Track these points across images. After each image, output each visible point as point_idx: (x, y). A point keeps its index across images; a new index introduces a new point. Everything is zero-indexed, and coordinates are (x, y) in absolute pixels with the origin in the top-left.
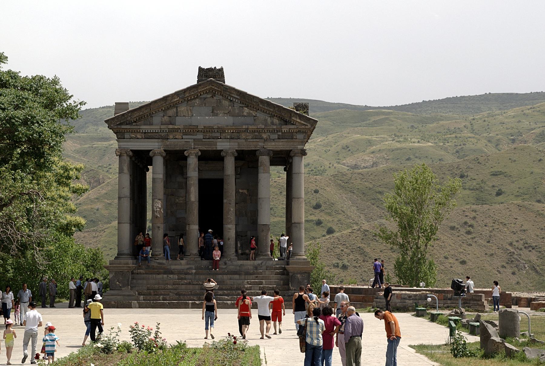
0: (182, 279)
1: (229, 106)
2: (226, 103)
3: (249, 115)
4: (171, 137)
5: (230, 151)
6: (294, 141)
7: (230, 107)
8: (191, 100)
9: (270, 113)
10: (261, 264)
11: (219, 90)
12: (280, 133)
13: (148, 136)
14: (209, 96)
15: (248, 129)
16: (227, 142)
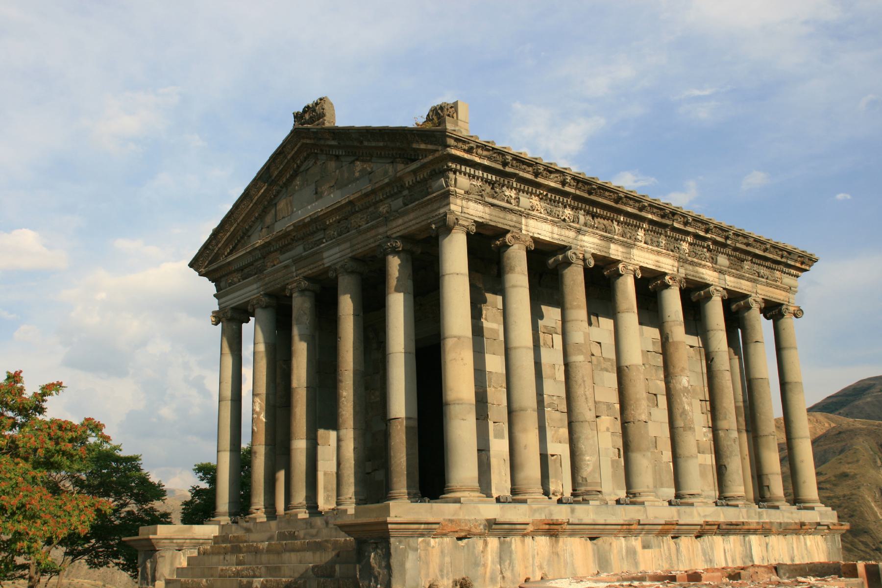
2: (332, 165)
5: (339, 265)
12: (406, 192)
15: (351, 203)
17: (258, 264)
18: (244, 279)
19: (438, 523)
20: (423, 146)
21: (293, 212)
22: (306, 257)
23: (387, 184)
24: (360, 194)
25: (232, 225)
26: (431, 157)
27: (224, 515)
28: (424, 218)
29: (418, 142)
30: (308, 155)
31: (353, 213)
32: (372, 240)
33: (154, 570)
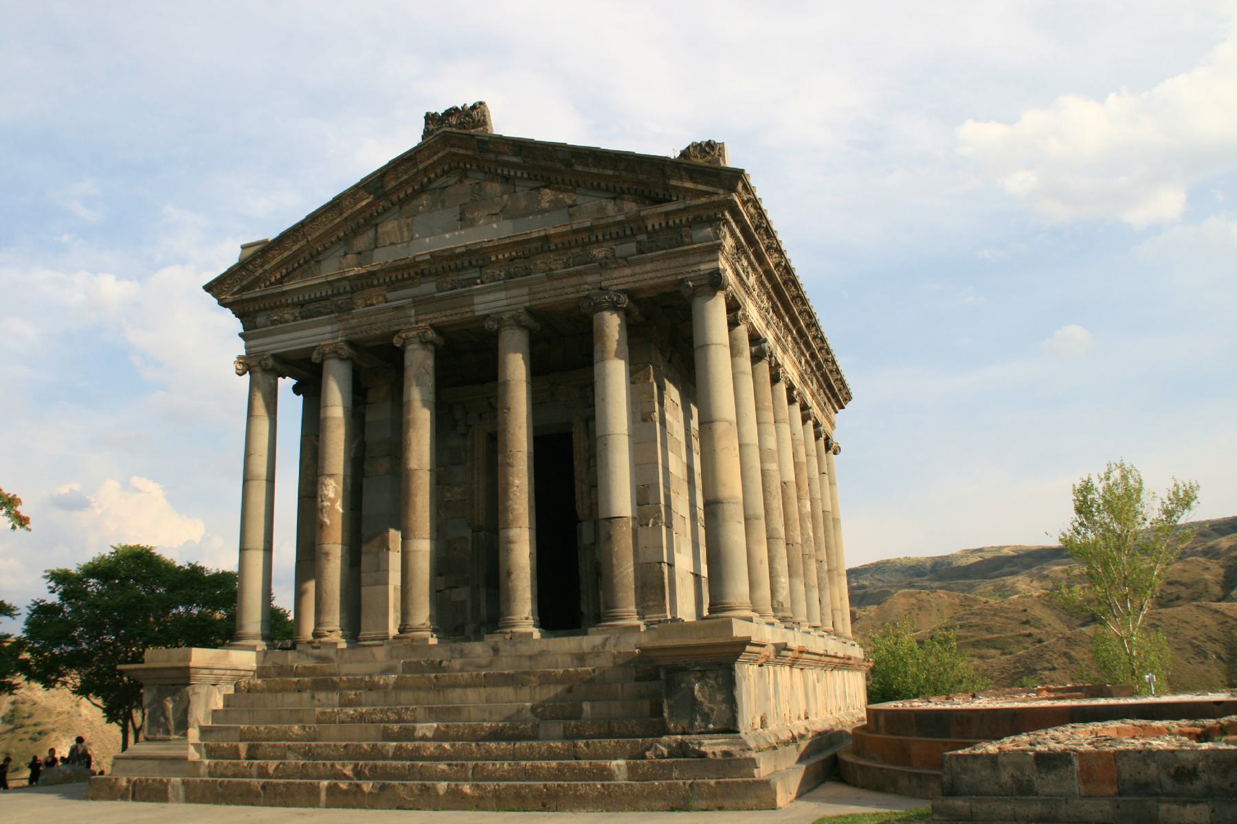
0: (350, 703)
1: (503, 193)
2: (494, 188)
3: (556, 205)
4: (360, 302)
6: (686, 254)
7: (506, 197)
8: (409, 198)
9: (611, 185)
10: (604, 645)
11: (470, 153)
12: (643, 237)
13: (308, 308)
14: (452, 181)
15: (546, 238)
16: (501, 290)
17: (340, 300)
18: (303, 318)
19: (763, 646)
20: (689, 185)
21: (412, 238)
22: (442, 299)
23: (619, 223)
24: (569, 228)
25: (296, 242)
26: (704, 200)
27: (254, 637)
28: (672, 271)
29: (681, 179)
30: (451, 169)
31: (543, 251)
32: (571, 290)
33: (186, 712)
